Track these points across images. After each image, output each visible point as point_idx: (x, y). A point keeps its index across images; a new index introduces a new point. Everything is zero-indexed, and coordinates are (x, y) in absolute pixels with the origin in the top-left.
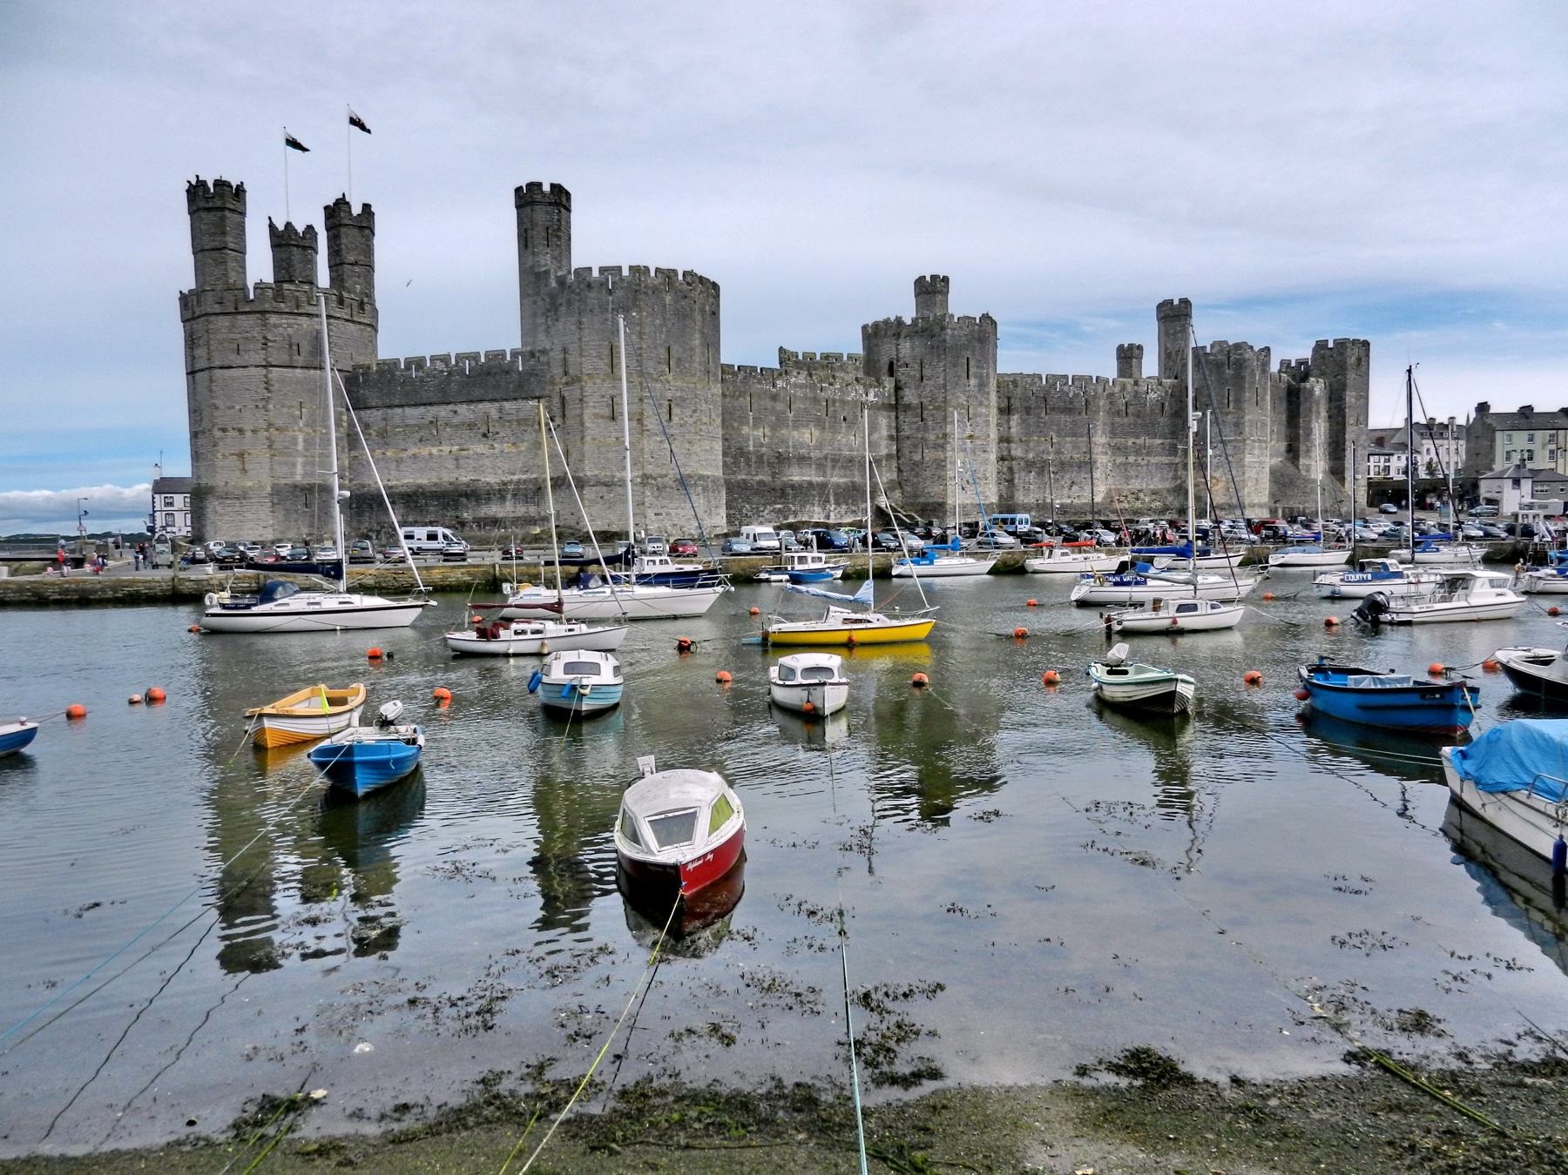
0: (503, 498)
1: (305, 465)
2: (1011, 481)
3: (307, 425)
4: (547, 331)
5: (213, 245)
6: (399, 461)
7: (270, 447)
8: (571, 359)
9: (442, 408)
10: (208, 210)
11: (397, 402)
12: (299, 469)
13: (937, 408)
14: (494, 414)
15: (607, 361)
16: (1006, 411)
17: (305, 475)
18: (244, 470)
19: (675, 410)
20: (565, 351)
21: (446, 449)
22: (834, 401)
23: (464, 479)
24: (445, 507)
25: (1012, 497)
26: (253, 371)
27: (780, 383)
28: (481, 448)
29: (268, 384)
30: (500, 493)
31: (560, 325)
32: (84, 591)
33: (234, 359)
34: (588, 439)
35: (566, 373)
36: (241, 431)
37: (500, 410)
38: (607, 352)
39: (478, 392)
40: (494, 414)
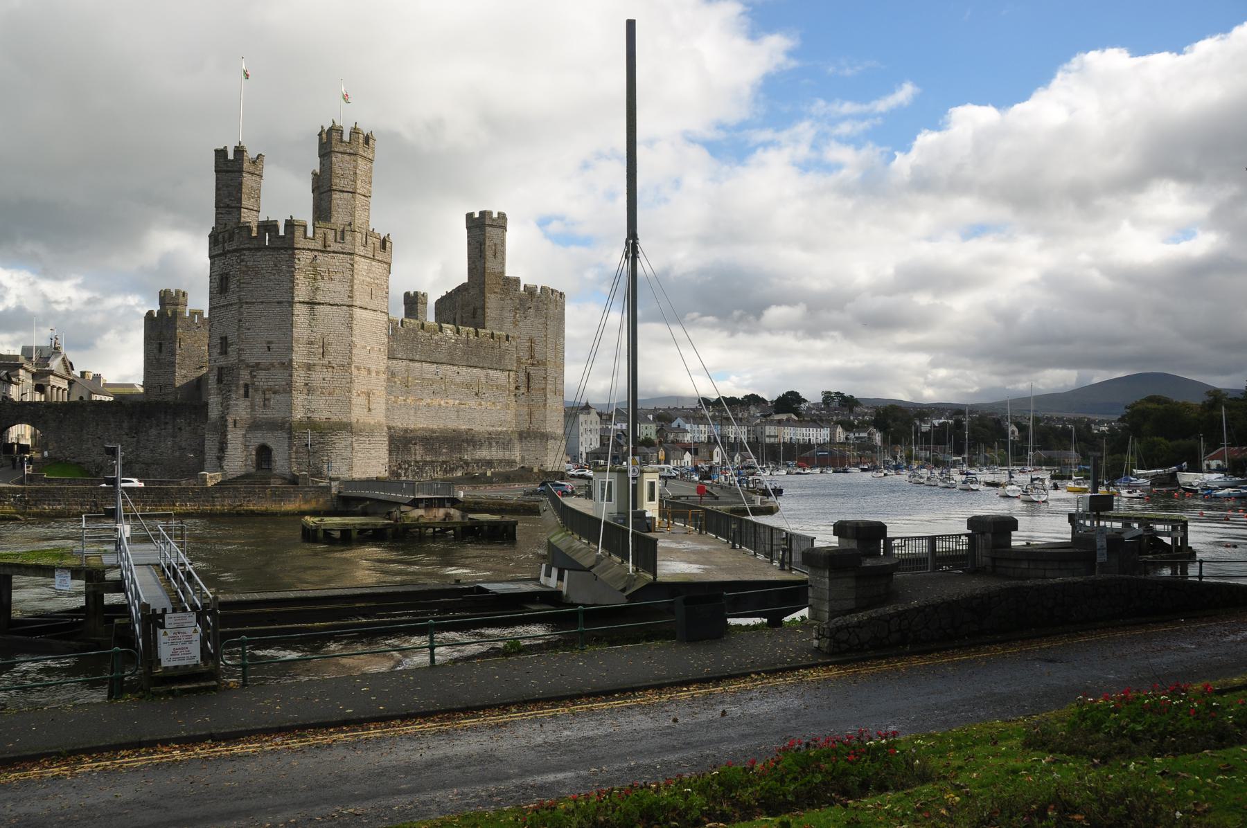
4: (515, 323)
6: (417, 409)
8: (537, 348)
9: (449, 367)
11: (417, 358)
14: (483, 379)
20: (532, 341)
21: (451, 402)
23: (464, 427)
24: (452, 450)
28: (472, 403)
30: (492, 439)
31: (528, 322)
37: (487, 376)
39: (474, 360)
40: (483, 379)
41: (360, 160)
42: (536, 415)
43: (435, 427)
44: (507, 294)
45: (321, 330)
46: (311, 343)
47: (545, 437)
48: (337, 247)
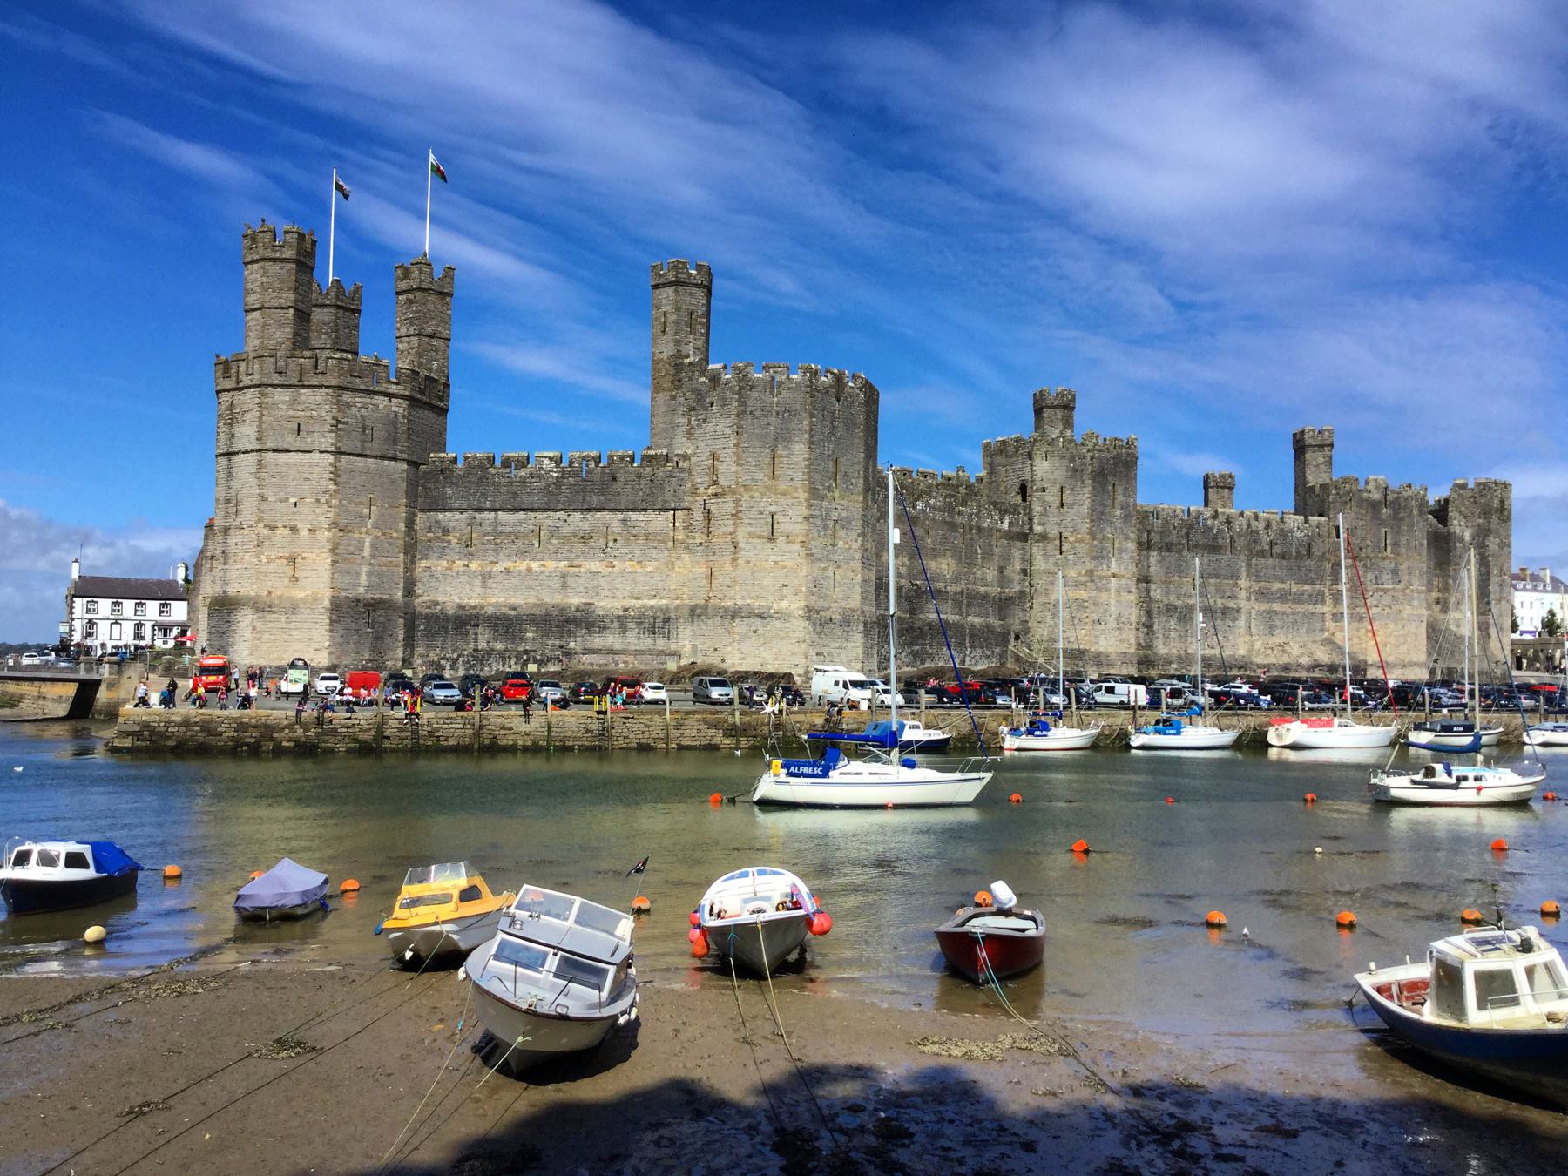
0: (624, 629)
1: (369, 575)
2: (1150, 627)
3: (375, 527)
4: (690, 434)
5: (275, 303)
6: (486, 577)
7: (332, 550)
8: (721, 467)
10: (275, 260)
11: (488, 505)
12: (363, 580)
13: (1081, 541)
15: (769, 471)
16: (1145, 546)
17: (369, 587)
18: (295, 579)
19: (841, 533)
21: (551, 565)
22: (971, 528)
23: (575, 601)
25: (1149, 647)
26: (316, 456)
27: (919, 505)
28: (595, 566)
29: (336, 476)
30: (622, 621)
31: (709, 427)
32: (266, 726)
33: (290, 440)
34: (741, 561)
35: (715, 482)
36: (294, 529)
37: (624, 522)
38: (768, 460)
41: (268, 265)
42: (720, 579)
43: (518, 600)
44: (678, 388)
45: (235, 485)
46: (228, 501)
47: (735, 614)
48: (246, 381)
